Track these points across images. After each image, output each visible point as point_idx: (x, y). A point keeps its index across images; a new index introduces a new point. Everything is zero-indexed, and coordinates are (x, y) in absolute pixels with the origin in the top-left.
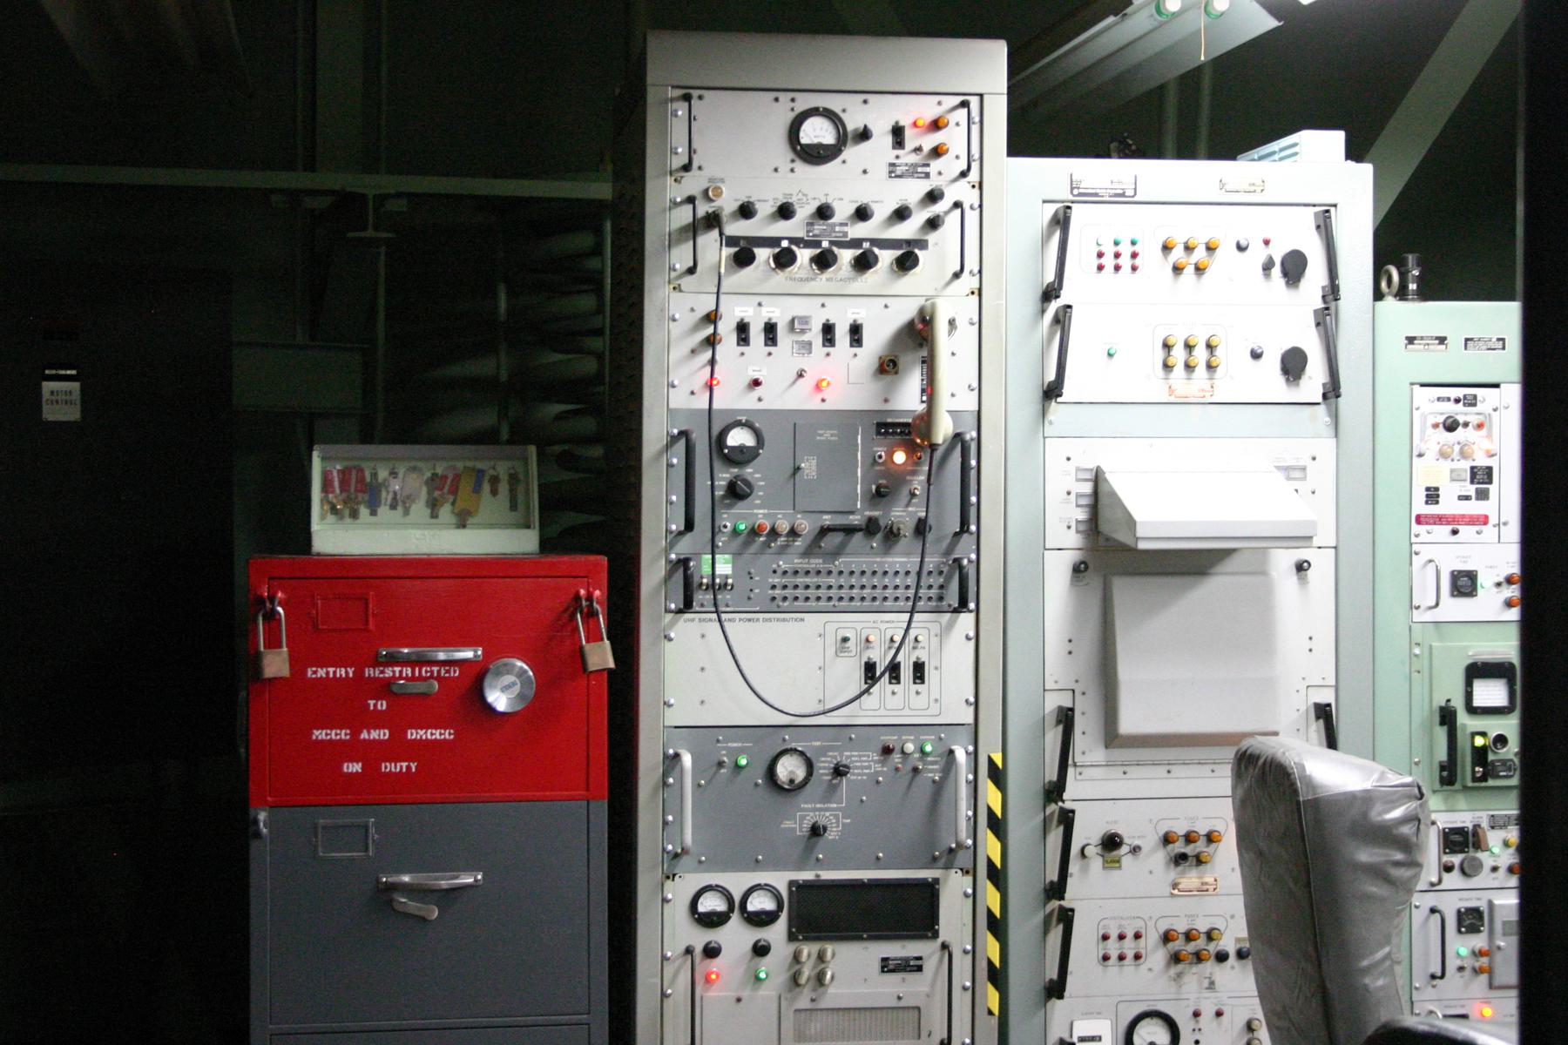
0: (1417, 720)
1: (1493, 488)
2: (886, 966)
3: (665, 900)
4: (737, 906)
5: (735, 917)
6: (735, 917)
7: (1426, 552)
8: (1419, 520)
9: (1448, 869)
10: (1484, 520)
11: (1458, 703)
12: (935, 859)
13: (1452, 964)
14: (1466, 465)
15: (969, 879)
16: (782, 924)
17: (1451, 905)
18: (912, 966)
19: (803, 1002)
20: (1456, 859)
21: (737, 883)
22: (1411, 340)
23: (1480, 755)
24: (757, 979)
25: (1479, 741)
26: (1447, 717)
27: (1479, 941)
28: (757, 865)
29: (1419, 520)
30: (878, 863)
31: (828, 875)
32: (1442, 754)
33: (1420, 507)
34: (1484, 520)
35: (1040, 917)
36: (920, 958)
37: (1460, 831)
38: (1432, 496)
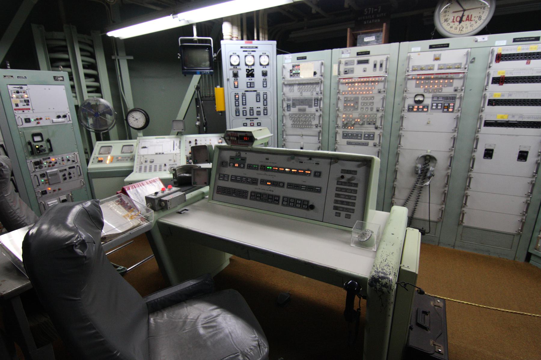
0: (24, 145)
1: (30, 103)
7: (18, 115)
8: (15, 110)
9: (36, 168)
10: (29, 109)
11: (31, 141)
13: (41, 184)
14: (23, 99)
17: (38, 174)
20: (38, 166)
22: (5, 76)
23: (38, 149)
25: (37, 147)
26: (30, 143)
27: (46, 178)
29: (15, 110)
32: (30, 150)
33: (14, 107)
34: (29, 109)
37: (38, 162)
38: (17, 105)
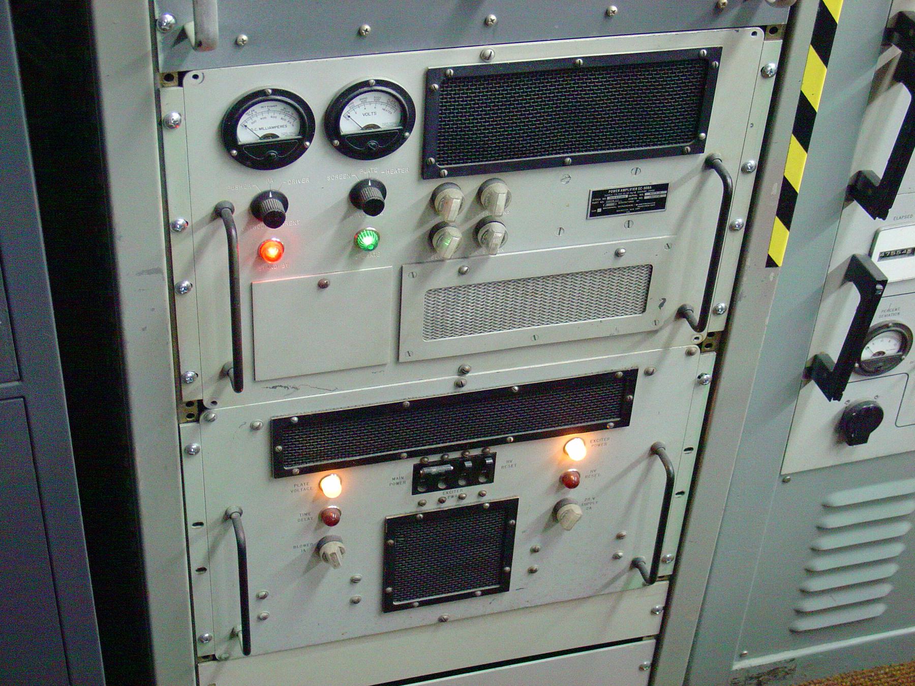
2: (602, 204)
3: (163, 124)
4: (322, 125)
5: (316, 148)
6: (316, 148)
12: (718, 9)
15: (777, 44)
16: (408, 153)
18: (651, 200)
19: (445, 277)
21: (316, 80)
24: (357, 246)
28: (360, 42)
30: (607, 23)
31: (506, 54)
35: (870, 75)
36: (664, 187)
